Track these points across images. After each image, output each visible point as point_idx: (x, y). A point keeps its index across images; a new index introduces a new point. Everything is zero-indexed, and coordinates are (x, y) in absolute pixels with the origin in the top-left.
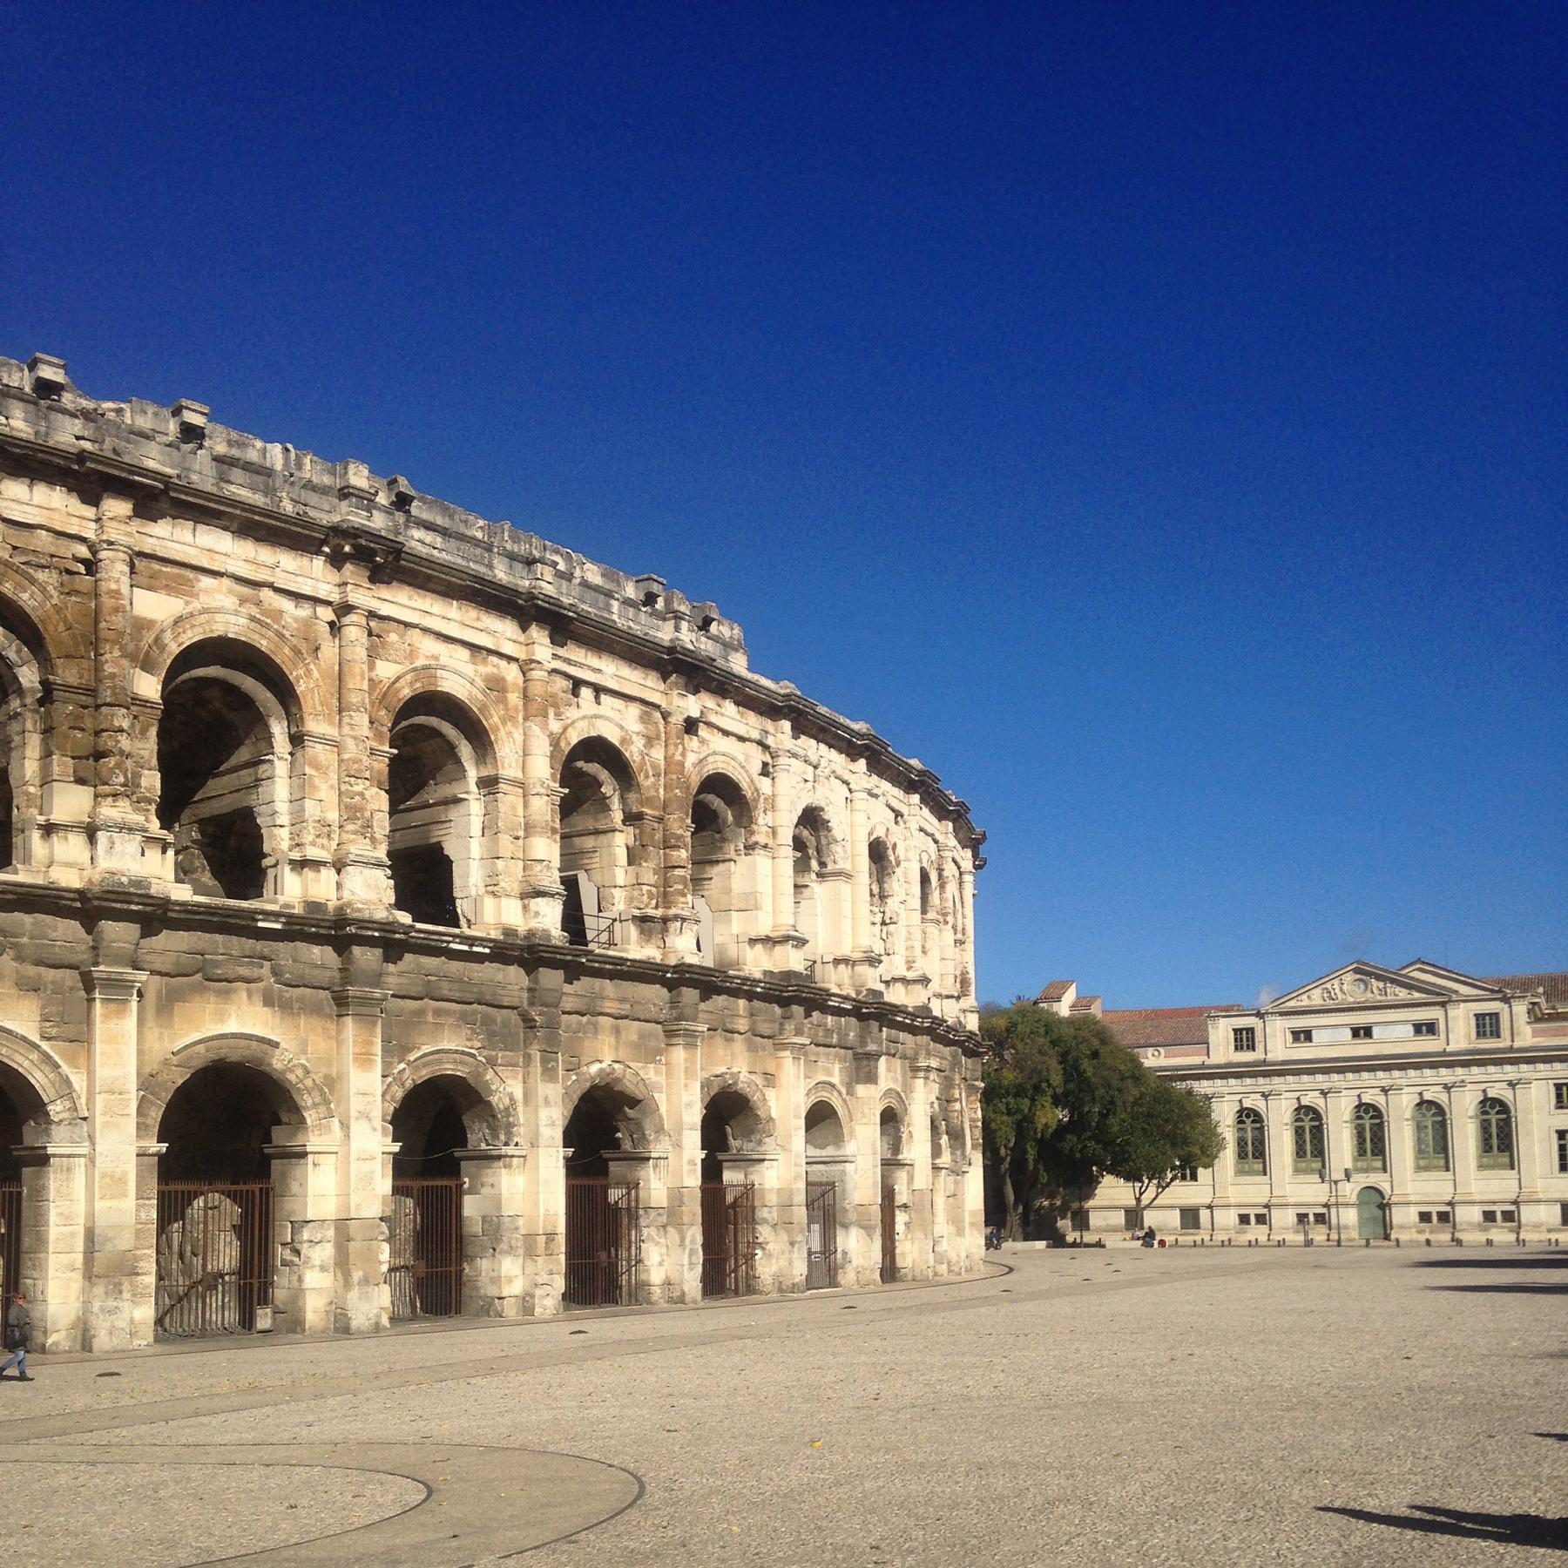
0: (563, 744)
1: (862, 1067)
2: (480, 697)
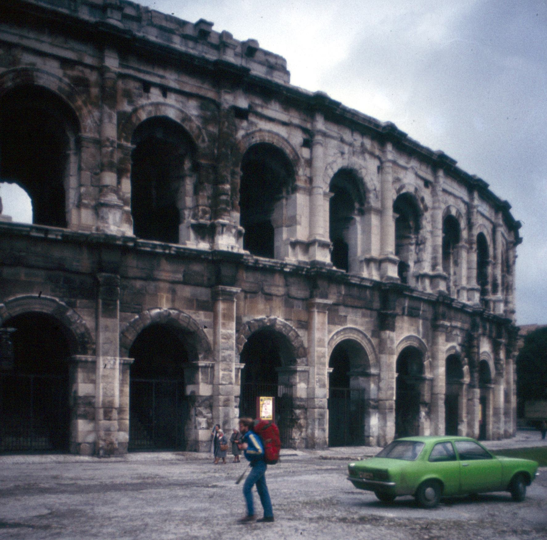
0: (134, 119)
1: (384, 322)
2: (67, 88)
